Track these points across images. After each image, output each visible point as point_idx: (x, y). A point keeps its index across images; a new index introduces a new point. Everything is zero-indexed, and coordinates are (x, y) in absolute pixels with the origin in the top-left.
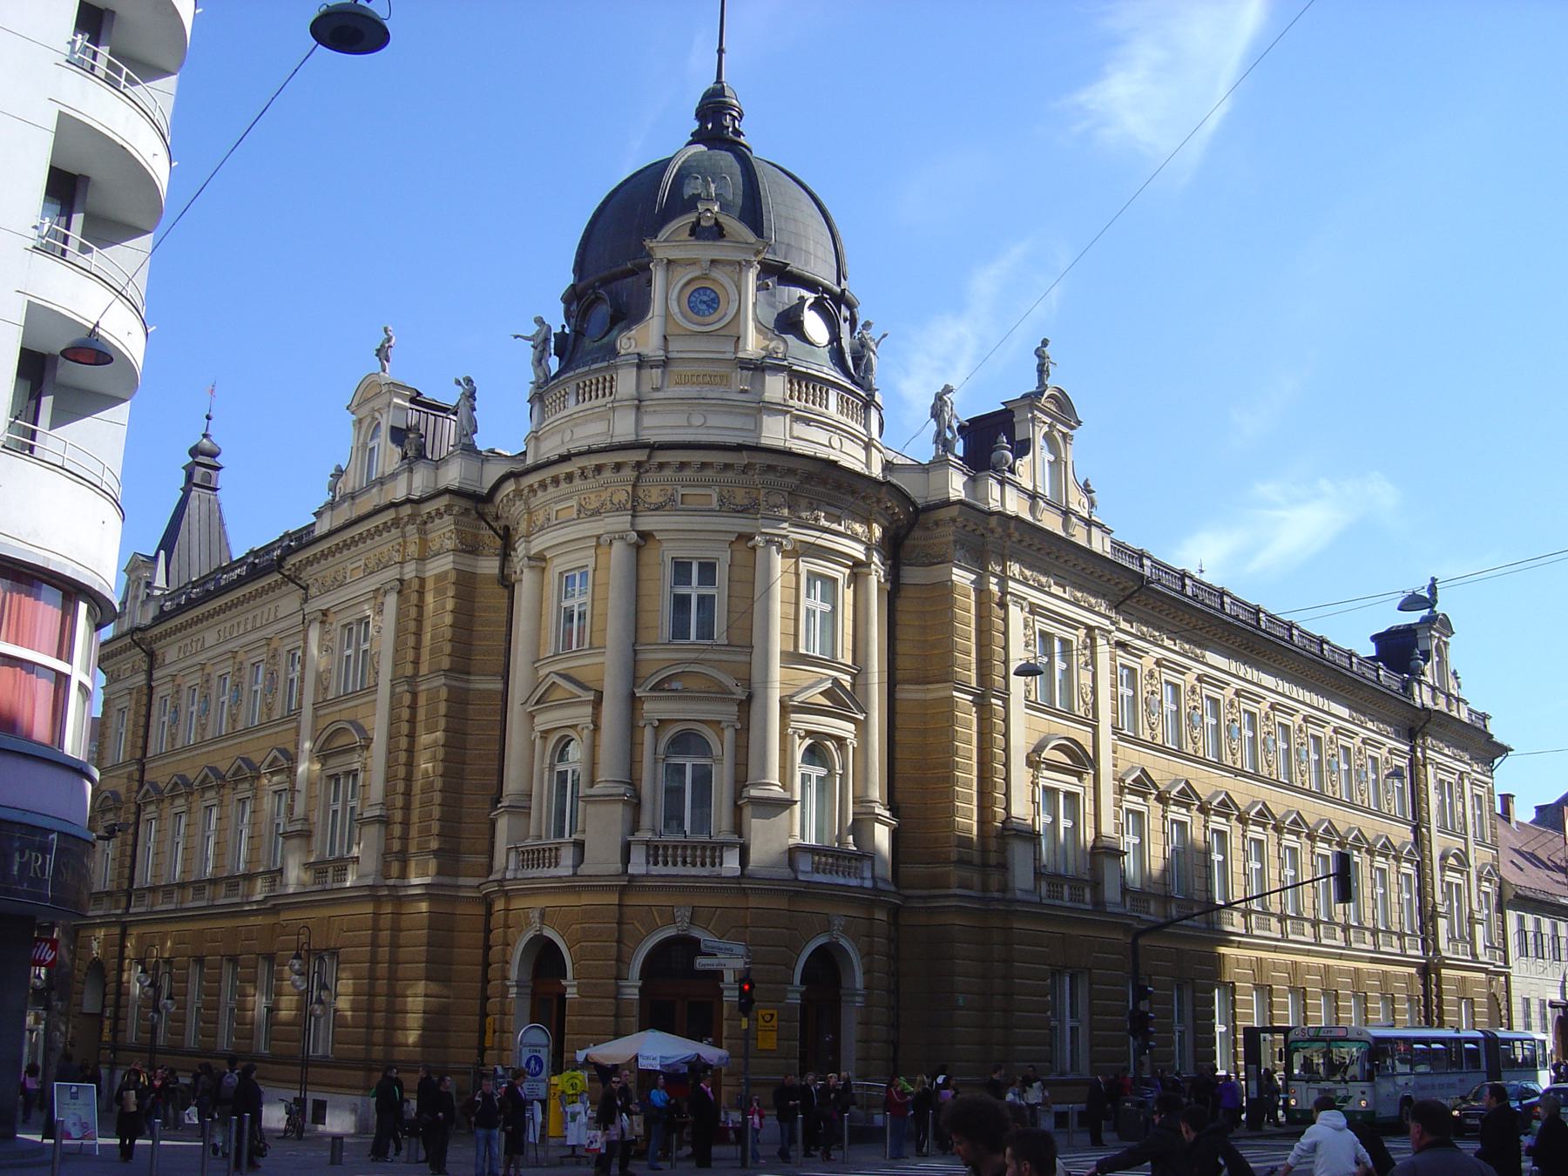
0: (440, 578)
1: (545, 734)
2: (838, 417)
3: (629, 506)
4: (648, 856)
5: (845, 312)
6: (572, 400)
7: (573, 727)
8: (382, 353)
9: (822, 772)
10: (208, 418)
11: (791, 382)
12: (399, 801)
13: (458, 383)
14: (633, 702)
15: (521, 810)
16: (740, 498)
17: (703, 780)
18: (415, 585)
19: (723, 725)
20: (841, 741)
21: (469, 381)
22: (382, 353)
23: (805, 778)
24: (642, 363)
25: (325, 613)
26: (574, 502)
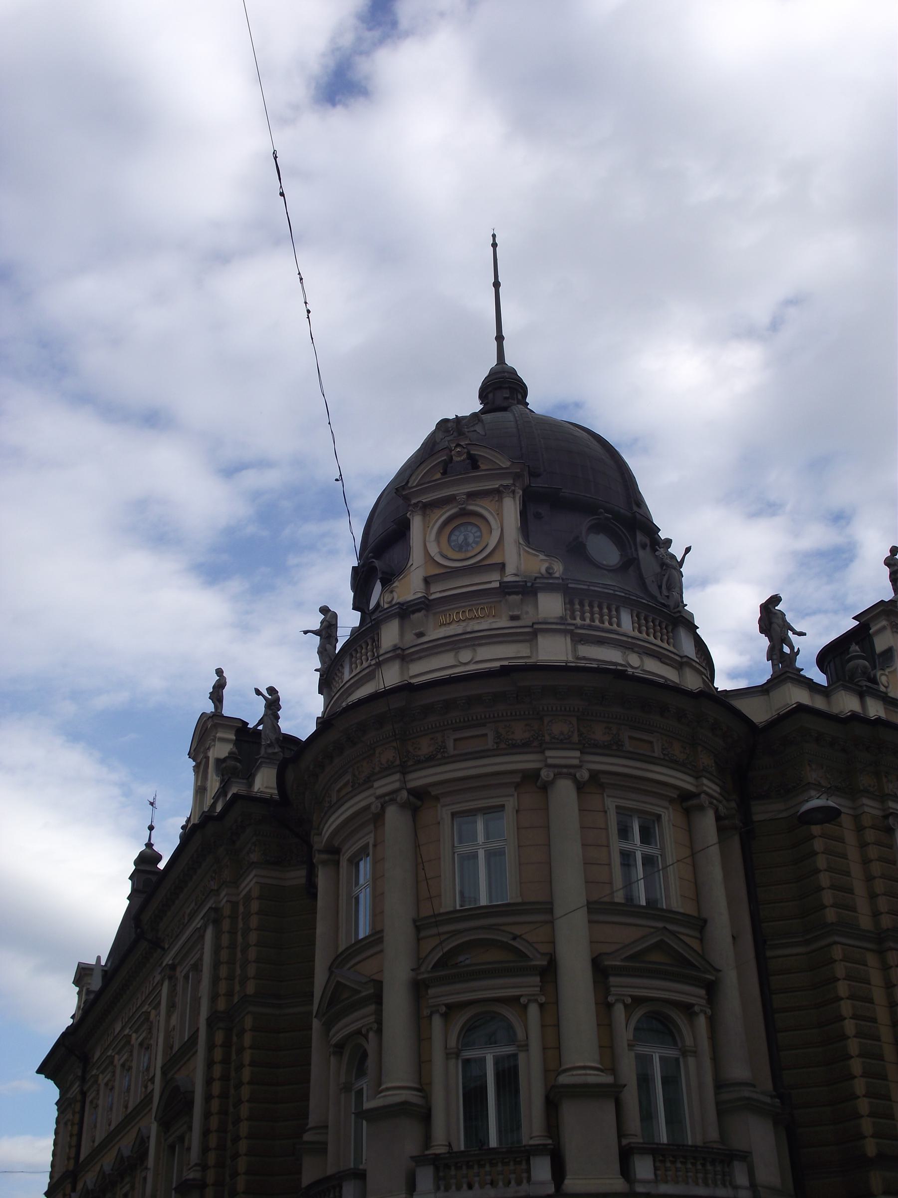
0: (248, 898)
1: (339, 1048)
2: (636, 634)
3: (398, 762)
4: (437, 1179)
5: (640, 537)
6: (346, 671)
7: (358, 1032)
8: (217, 694)
9: (672, 1053)
10: (151, 828)
11: (571, 603)
12: (212, 1158)
13: (258, 692)
14: (418, 988)
15: (321, 1149)
16: (519, 732)
17: (508, 1077)
18: (227, 911)
19: (523, 1000)
20: (688, 1009)
21: (272, 690)
22: (217, 694)
23: (644, 1062)
24: (404, 611)
25: (173, 967)
26: (348, 777)
